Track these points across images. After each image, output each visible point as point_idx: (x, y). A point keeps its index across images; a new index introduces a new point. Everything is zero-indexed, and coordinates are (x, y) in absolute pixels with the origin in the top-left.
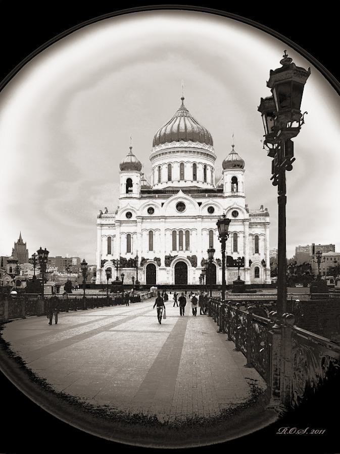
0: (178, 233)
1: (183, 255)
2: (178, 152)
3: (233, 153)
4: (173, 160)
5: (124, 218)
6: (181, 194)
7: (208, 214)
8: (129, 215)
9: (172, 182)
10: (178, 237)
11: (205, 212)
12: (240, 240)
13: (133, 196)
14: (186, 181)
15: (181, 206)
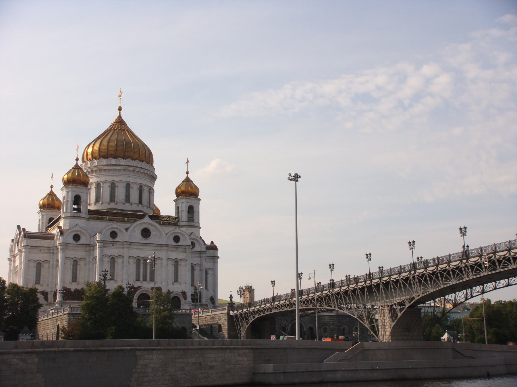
0: (142, 261)
1: (147, 286)
2: (125, 170)
3: (188, 181)
4: (116, 179)
5: (71, 241)
6: (147, 219)
7: (174, 243)
8: (77, 237)
9: (116, 204)
10: (142, 265)
11: (172, 242)
12: (197, 273)
13: (84, 215)
14: (131, 204)
15: (146, 233)
